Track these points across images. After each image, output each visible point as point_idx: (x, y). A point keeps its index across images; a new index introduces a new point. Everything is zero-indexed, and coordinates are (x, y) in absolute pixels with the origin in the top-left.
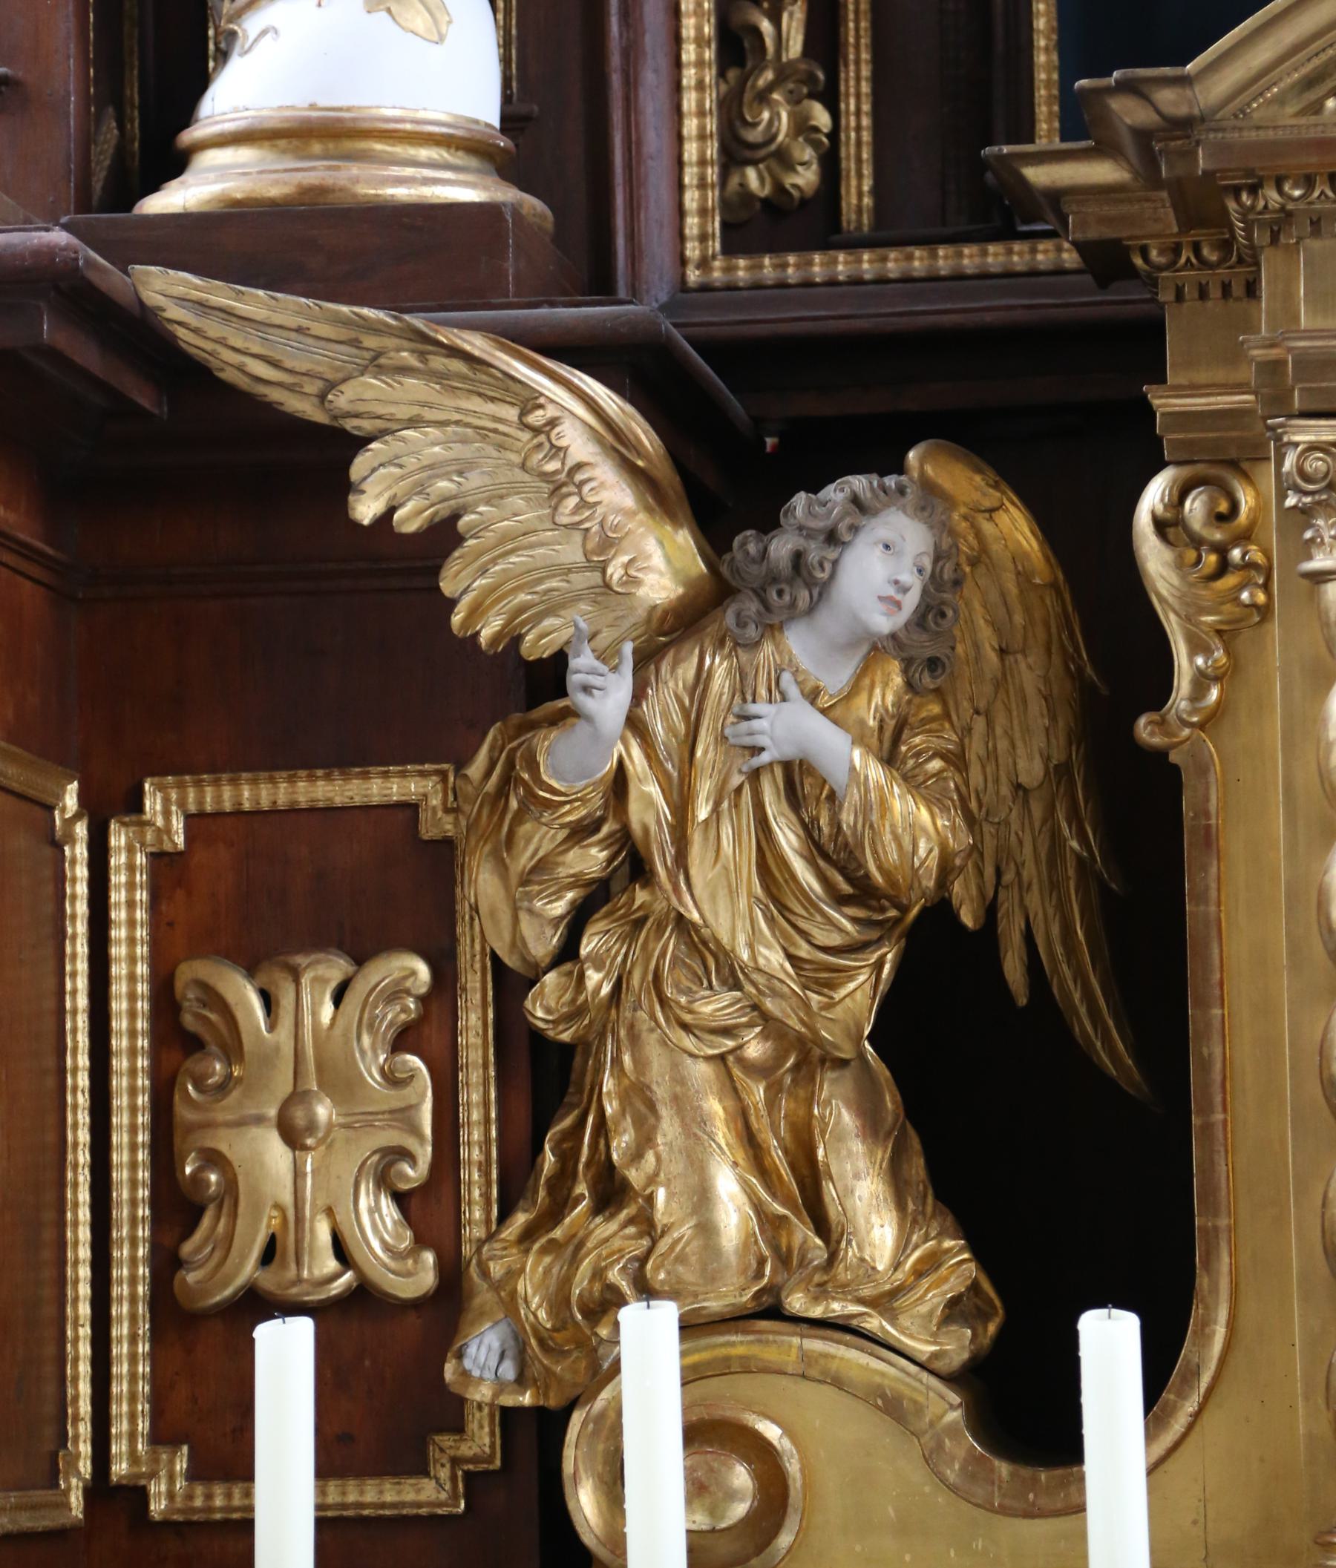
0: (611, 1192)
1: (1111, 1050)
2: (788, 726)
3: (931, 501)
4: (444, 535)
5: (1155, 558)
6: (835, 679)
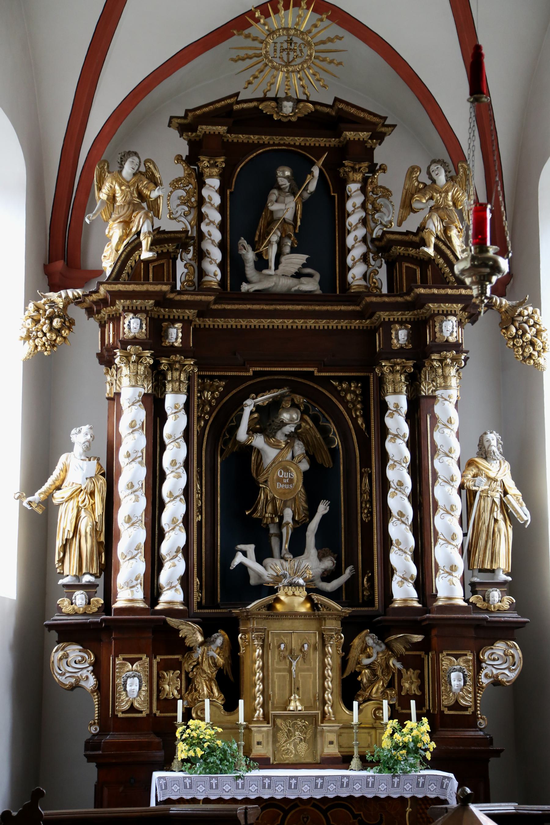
0: (196, 690)
1: (232, 678)
2: (211, 653)
3: (223, 636)
4: (185, 637)
6: (215, 649)
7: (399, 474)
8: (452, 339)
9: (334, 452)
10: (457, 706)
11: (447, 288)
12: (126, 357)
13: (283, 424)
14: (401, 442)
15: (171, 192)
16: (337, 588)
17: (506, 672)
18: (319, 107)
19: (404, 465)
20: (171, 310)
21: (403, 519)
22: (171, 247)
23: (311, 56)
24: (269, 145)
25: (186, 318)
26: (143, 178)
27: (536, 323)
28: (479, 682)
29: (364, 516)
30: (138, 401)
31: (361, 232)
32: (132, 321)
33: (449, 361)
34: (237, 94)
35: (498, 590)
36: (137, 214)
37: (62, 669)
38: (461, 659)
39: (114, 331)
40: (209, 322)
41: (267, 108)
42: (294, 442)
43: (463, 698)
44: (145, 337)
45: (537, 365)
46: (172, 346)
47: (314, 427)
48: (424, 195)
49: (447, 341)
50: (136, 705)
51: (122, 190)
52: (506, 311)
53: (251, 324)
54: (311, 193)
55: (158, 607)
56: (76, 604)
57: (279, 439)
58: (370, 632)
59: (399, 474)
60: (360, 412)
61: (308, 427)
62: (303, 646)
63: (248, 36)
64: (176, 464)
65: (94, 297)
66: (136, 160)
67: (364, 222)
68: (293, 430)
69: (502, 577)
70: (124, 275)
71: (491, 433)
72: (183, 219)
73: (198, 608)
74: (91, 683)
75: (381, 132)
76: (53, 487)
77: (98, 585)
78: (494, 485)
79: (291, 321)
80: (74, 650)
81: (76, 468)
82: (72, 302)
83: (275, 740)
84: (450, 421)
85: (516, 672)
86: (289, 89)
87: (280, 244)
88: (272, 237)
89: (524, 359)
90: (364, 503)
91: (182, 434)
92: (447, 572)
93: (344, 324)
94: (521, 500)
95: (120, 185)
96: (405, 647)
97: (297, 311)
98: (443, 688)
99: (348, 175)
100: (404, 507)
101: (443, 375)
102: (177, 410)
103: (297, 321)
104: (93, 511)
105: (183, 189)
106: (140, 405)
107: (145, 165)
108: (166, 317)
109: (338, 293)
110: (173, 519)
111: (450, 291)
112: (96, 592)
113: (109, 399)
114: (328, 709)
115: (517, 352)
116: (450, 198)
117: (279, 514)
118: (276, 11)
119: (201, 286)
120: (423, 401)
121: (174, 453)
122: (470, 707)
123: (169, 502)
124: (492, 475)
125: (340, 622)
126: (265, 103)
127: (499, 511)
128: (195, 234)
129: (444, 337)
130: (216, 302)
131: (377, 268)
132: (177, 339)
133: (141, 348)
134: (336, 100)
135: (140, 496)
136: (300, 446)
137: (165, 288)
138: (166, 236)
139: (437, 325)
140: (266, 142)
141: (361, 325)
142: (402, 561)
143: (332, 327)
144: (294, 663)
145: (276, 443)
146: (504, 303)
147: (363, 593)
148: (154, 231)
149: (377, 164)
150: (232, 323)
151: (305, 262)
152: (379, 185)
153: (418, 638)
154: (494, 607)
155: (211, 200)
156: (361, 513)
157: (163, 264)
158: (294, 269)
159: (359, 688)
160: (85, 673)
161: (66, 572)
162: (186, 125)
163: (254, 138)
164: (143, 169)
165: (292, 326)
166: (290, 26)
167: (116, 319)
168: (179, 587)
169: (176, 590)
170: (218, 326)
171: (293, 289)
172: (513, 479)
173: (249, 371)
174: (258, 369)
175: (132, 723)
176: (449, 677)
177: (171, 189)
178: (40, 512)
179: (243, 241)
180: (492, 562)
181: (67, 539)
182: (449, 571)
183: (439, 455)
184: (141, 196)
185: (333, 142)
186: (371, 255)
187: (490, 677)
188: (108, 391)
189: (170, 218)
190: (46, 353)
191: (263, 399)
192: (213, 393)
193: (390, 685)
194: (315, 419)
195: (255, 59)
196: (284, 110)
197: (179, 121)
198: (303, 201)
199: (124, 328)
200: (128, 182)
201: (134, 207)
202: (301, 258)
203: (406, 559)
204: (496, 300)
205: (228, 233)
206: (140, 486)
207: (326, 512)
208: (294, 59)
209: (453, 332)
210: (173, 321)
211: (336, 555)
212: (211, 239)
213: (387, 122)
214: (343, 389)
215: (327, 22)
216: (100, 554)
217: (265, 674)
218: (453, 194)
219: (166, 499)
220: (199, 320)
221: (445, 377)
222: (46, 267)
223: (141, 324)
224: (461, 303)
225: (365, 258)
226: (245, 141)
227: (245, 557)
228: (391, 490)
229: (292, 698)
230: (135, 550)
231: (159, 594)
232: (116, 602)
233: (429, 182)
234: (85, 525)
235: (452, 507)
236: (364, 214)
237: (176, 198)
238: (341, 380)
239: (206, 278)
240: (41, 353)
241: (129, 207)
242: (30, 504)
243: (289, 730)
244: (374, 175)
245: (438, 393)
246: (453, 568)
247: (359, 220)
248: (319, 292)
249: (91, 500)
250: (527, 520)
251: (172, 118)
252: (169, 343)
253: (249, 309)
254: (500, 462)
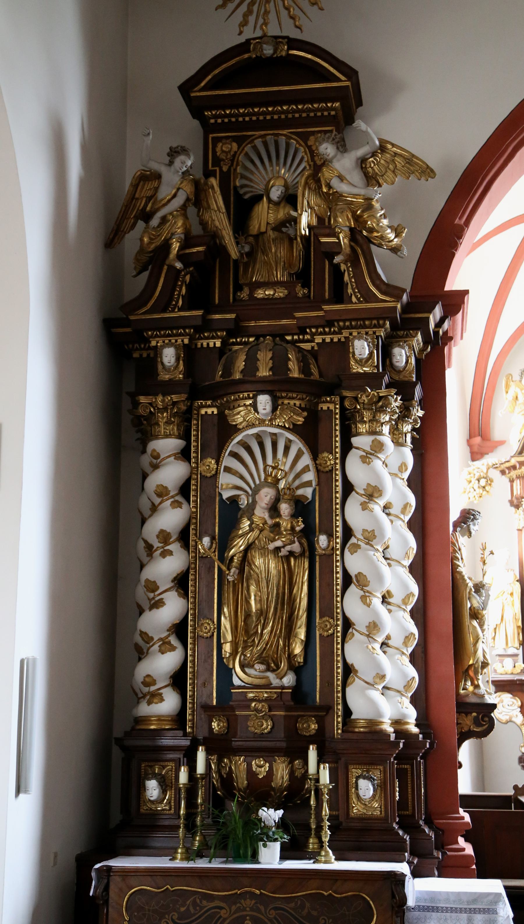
104: (513, 605)
113: (519, 530)
222: (468, 441)
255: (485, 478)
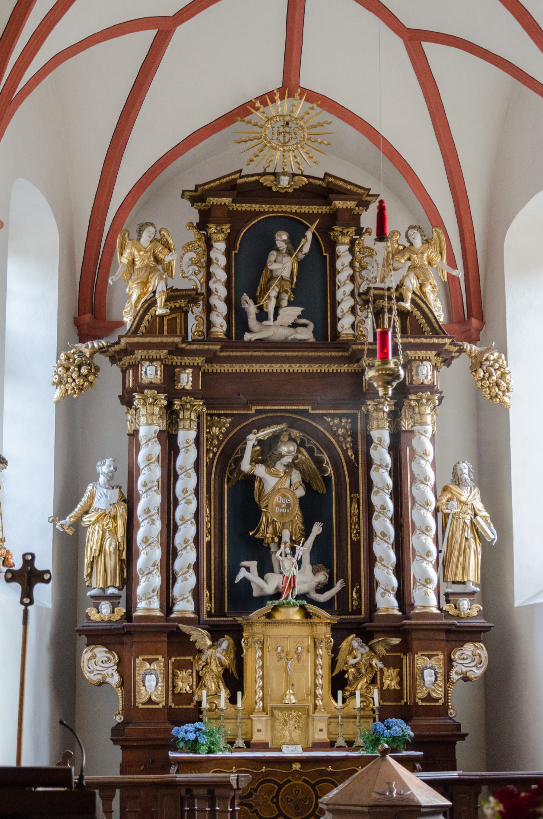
2: (218, 655)
3: (228, 640)
4: (196, 641)
5: (243, 644)
6: (221, 651)
7: (383, 500)
8: (427, 382)
9: (327, 480)
10: (429, 698)
11: (422, 337)
12: (144, 399)
13: (281, 456)
14: (384, 471)
15: (184, 254)
16: (328, 599)
17: (474, 669)
18: (311, 180)
19: (387, 491)
20: (182, 358)
21: (386, 538)
22: (182, 303)
23: (304, 138)
24: (269, 212)
25: (196, 364)
26: (159, 244)
27: (500, 367)
28: (450, 678)
29: (353, 535)
30: (154, 437)
31: (349, 287)
32: (148, 368)
33: (424, 401)
34: (240, 171)
35: (467, 599)
36: (153, 276)
37: (90, 667)
38: (433, 659)
39: (133, 376)
40: (217, 368)
41: (267, 181)
42: (292, 471)
43: (434, 691)
44: (160, 382)
45: (502, 402)
46: (184, 389)
47: (309, 458)
48: (403, 256)
49: (422, 383)
50: (153, 698)
51: (140, 255)
52: (476, 356)
53: (253, 368)
54: (305, 254)
55: (173, 616)
56: (102, 613)
57: (278, 469)
58: (356, 637)
59: (383, 500)
60: (350, 445)
61: (304, 458)
62: (297, 649)
63: (249, 122)
64: (187, 492)
65: (117, 348)
66: (152, 229)
67: (352, 278)
68: (291, 461)
69: (472, 588)
70: (142, 328)
71: (464, 462)
72: (193, 277)
73: (207, 617)
74: (115, 680)
75: (367, 201)
76: (82, 512)
77: (120, 597)
78: (465, 508)
79: (288, 365)
80: (101, 652)
81: (101, 496)
82: (97, 352)
83: (273, 729)
84: (425, 453)
85: (483, 669)
86: (286, 165)
87: (278, 298)
88: (271, 293)
89: (491, 398)
90: (353, 524)
91: (192, 466)
92: (423, 584)
93: (334, 368)
94: (489, 521)
95: (139, 251)
96: (385, 649)
97: (293, 357)
98: (417, 683)
99: (337, 238)
100: (386, 527)
101: (419, 413)
102: (188, 445)
103: (293, 365)
104: (116, 532)
105: (194, 252)
106: (155, 441)
107: (160, 233)
108: (179, 364)
109: (329, 341)
110: (185, 540)
111: (424, 340)
112: (119, 603)
114: (319, 702)
115: (485, 392)
116: (425, 258)
117: (278, 534)
118: (273, 101)
119: (210, 336)
120: (403, 435)
121: (186, 483)
122: (441, 699)
123: (182, 524)
124: (463, 499)
125: (329, 628)
126: (264, 178)
127: (469, 531)
128: (204, 291)
129: (420, 379)
130: (221, 350)
131: (364, 319)
132: (187, 383)
133: (156, 392)
134: (326, 174)
135: (156, 519)
136: (297, 475)
137: (178, 340)
138: (178, 293)
139: (414, 368)
140: (266, 210)
141: (350, 369)
142: (385, 575)
143: (325, 370)
144: (290, 663)
145: (276, 473)
146: (474, 349)
147: (352, 603)
148: (167, 290)
149: (363, 228)
150: (237, 368)
151: (300, 314)
152: (365, 246)
153: (396, 641)
154: (464, 615)
155: (218, 261)
156: (351, 533)
157: (177, 317)
158: (290, 321)
159: (347, 684)
160: (110, 671)
161: (94, 585)
162: (197, 196)
163: (256, 207)
164: (158, 237)
165: (289, 370)
166: (285, 113)
167: (135, 367)
168: (190, 598)
169: (188, 601)
170: (224, 370)
171: (289, 338)
172: (483, 503)
173: (251, 410)
174: (259, 408)
175: (150, 713)
176: (422, 674)
177: (183, 252)
178: (71, 533)
179: (245, 297)
180: (463, 575)
181: (93, 557)
182: (424, 583)
183: (416, 482)
184: (157, 260)
185: (325, 209)
186: (359, 307)
187: (460, 674)
188: (129, 428)
189: (183, 277)
190: (75, 396)
191: (265, 434)
192: (220, 428)
193: (373, 681)
194: (310, 451)
195: (256, 142)
196: (282, 183)
197: (191, 194)
198: (299, 260)
199: (141, 375)
200: (145, 248)
201: (150, 270)
202: (298, 310)
203: (388, 573)
204: (467, 347)
205: (233, 289)
206: (156, 511)
207: (320, 532)
208: (289, 141)
209: (427, 375)
210: (185, 367)
211: (329, 570)
212: (217, 295)
213: (371, 193)
214: (335, 425)
215: (318, 109)
216: (122, 570)
217: (265, 672)
218: (428, 255)
219: (179, 522)
220: (208, 365)
221: (421, 415)
223: (156, 371)
224: (435, 350)
225: (353, 310)
226: (248, 209)
227: (248, 571)
228: (375, 513)
229: (288, 692)
230: (152, 566)
231: (173, 604)
232: (135, 611)
233: (407, 245)
234: (109, 546)
235: (427, 527)
236: (351, 272)
237: (188, 260)
238: (333, 416)
239: (213, 329)
240: (71, 395)
241: (146, 270)
242: (62, 527)
243: (284, 719)
244: (360, 237)
245: (415, 428)
246: (428, 581)
247: (347, 277)
248: (313, 340)
249: (114, 524)
250: (494, 539)
251: (184, 191)
252: (181, 386)
253: (251, 356)
254: (471, 488)
255: (89, 365)
